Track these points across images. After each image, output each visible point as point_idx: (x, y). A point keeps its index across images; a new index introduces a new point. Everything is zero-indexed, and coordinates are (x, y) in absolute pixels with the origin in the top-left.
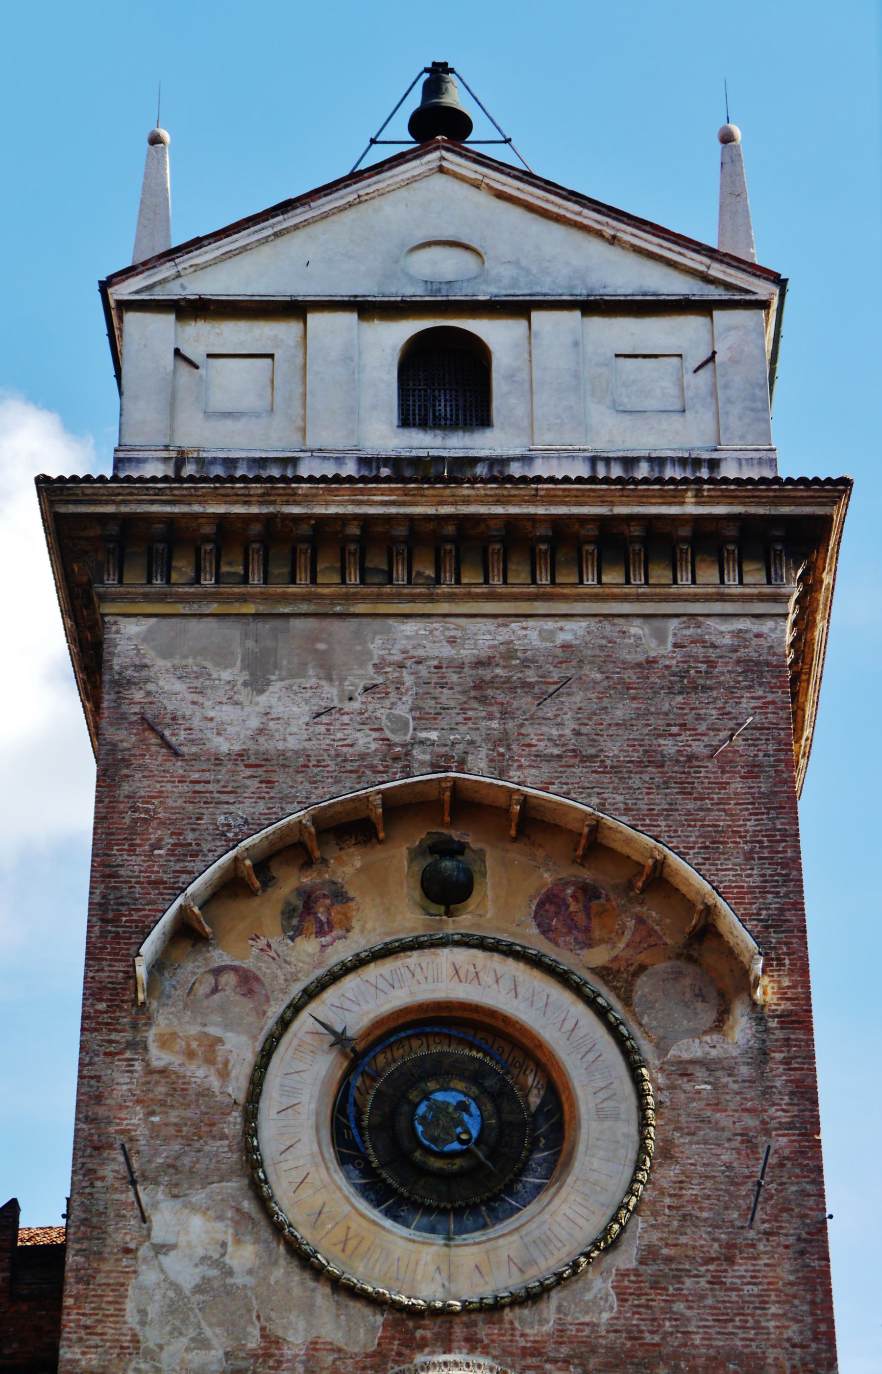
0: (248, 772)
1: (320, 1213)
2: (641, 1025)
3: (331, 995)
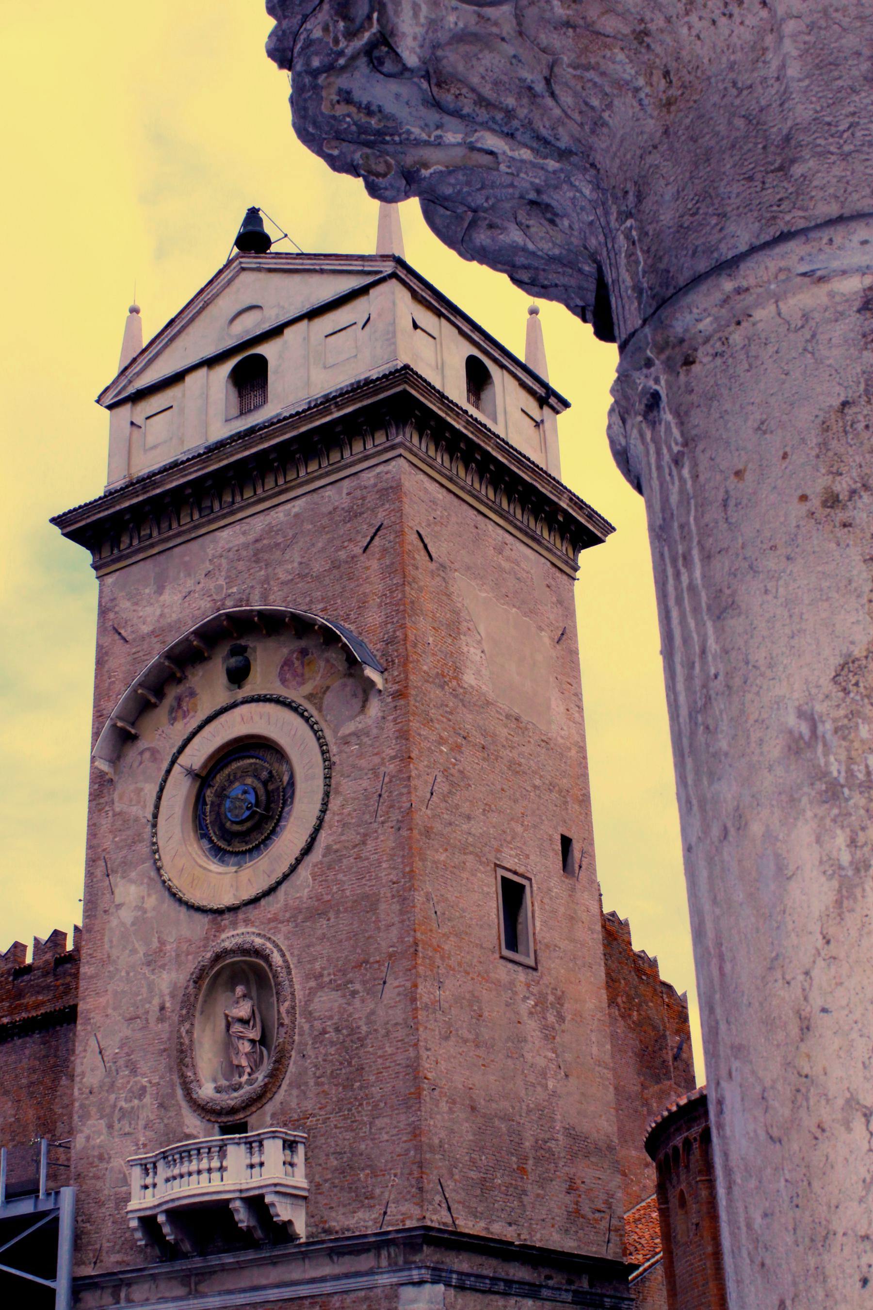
0: (156, 640)
3: (188, 750)
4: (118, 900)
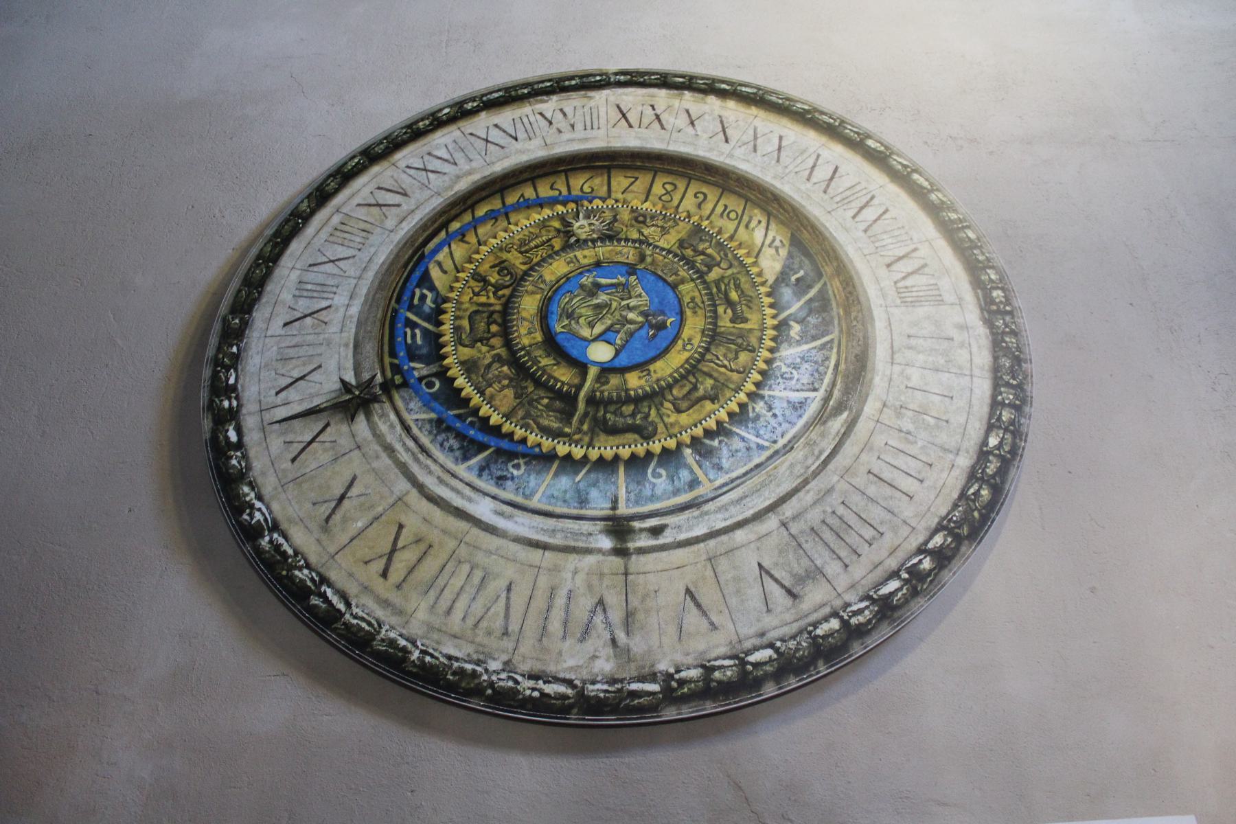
1: (342, 497)
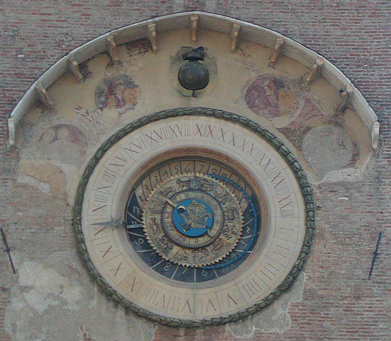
2: (308, 162)
4: (23, 281)
